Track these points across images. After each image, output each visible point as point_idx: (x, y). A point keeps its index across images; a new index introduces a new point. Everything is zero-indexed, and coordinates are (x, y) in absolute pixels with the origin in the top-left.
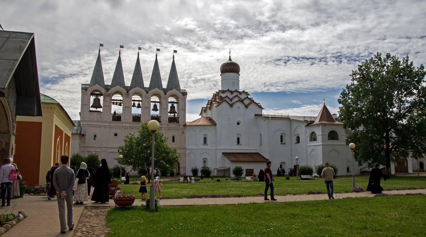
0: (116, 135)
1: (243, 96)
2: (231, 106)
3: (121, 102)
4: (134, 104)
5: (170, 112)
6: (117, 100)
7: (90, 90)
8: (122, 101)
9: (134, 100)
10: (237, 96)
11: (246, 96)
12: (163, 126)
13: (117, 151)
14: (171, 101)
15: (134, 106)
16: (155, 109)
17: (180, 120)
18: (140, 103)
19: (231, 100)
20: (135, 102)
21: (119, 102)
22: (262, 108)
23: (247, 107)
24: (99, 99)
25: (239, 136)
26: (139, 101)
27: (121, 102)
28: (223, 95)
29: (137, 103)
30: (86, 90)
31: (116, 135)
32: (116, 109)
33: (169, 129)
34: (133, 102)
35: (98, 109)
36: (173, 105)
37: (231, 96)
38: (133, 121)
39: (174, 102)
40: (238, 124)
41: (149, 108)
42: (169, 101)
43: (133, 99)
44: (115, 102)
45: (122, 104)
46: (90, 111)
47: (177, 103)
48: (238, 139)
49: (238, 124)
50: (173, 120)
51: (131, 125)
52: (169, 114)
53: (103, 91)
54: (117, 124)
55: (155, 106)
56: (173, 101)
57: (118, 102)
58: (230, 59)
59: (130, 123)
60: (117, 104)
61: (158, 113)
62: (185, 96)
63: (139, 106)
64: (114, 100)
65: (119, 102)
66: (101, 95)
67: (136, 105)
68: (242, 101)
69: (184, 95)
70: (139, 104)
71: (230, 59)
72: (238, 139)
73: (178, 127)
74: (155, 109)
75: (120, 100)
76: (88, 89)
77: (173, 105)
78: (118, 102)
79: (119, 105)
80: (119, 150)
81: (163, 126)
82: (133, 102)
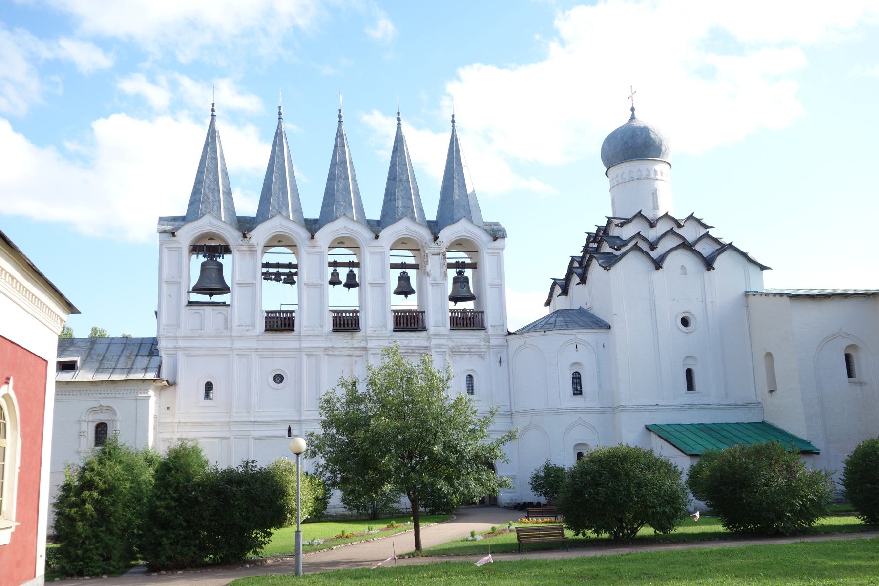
0: (279, 378)
1: (690, 233)
2: (658, 264)
3: (293, 271)
4: (335, 274)
5: (455, 299)
6: (278, 265)
7: (187, 234)
8: (296, 266)
9: (334, 264)
10: (671, 231)
11: (703, 232)
12: (434, 342)
13: (286, 433)
14: (454, 261)
15: (335, 281)
16: (404, 289)
17: (490, 319)
18: (356, 270)
19: (653, 246)
21: (286, 271)
22: (763, 268)
24: (220, 266)
26: (351, 264)
27: (293, 271)
28: (626, 233)
29: (343, 273)
30: (173, 235)
31: (279, 378)
32: (277, 297)
33: (456, 351)
34: (331, 269)
35: (216, 298)
37: (652, 234)
38: (334, 330)
39: (464, 265)
40: (685, 322)
41: (383, 286)
42: (449, 261)
43: (332, 259)
45: (295, 278)
46: (191, 303)
47: (473, 266)
48: (689, 373)
50: (461, 322)
51: (328, 344)
52: (451, 305)
53: (231, 236)
54: (282, 340)
55: (404, 279)
56: (460, 261)
57: (282, 270)
58: (633, 118)
59: (327, 338)
60: (278, 279)
62: (499, 243)
63: (351, 283)
64: (266, 265)
65: (286, 271)
66: (227, 250)
67: (343, 278)
68: (687, 246)
69: (495, 239)
70: (351, 276)
71: (633, 118)
72: (689, 373)
73: (483, 343)
74: (404, 289)
75: (290, 265)
77: (460, 273)
78: (282, 270)
79: (285, 282)
80: (289, 430)
81: (434, 342)
82: (331, 269)
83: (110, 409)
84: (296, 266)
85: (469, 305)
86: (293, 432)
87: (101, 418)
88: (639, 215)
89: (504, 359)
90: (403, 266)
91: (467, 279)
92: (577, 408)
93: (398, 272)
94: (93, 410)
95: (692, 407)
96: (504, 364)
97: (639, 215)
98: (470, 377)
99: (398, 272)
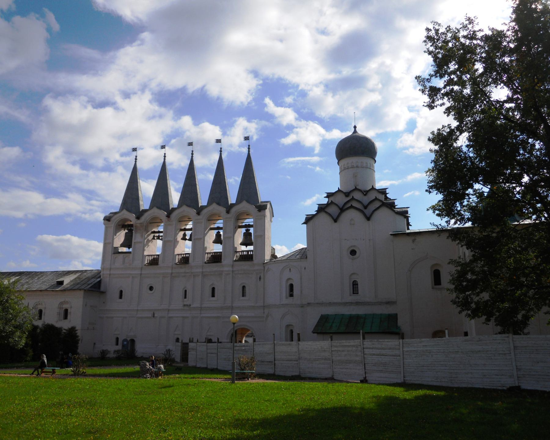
0: (151, 288)
5: (244, 244)
8: (161, 232)
15: (184, 238)
20: (187, 232)
23: (368, 219)
25: (354, 278)
36: (248, 231)
40: (353, 253)
44: (157, 235)
49: (353, 253)
55: (218, 235)
56: (247, 224)
61: (218, 248)
64: (154, 232)
67: (187, 237)
76: (112, 219)
77: (248, 231)
80: (154, 314)
83: (66, 303)
84: (161, 232)
85: (251, 248)
86: (156, 315)
87: (65, 306)
88: (356, 189)
89: (262, 277)
90: (218, 228)
91: (251, 233)
92: (287, 304)
93: (215, 232)
94: (61, 303)
95: (351, 304)
96: (262, 280)
97: (356, 189)
98: (244, 287)
99: (215, 232)
